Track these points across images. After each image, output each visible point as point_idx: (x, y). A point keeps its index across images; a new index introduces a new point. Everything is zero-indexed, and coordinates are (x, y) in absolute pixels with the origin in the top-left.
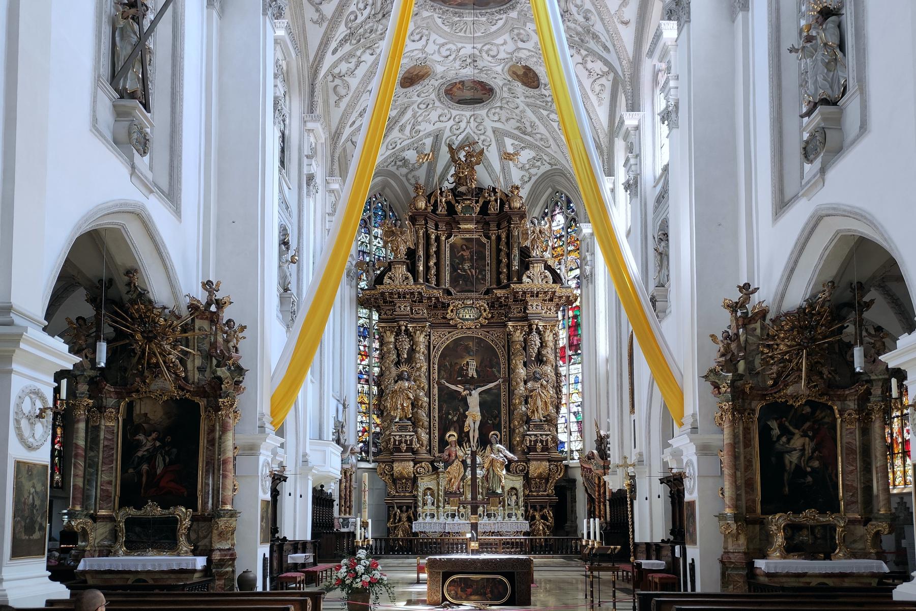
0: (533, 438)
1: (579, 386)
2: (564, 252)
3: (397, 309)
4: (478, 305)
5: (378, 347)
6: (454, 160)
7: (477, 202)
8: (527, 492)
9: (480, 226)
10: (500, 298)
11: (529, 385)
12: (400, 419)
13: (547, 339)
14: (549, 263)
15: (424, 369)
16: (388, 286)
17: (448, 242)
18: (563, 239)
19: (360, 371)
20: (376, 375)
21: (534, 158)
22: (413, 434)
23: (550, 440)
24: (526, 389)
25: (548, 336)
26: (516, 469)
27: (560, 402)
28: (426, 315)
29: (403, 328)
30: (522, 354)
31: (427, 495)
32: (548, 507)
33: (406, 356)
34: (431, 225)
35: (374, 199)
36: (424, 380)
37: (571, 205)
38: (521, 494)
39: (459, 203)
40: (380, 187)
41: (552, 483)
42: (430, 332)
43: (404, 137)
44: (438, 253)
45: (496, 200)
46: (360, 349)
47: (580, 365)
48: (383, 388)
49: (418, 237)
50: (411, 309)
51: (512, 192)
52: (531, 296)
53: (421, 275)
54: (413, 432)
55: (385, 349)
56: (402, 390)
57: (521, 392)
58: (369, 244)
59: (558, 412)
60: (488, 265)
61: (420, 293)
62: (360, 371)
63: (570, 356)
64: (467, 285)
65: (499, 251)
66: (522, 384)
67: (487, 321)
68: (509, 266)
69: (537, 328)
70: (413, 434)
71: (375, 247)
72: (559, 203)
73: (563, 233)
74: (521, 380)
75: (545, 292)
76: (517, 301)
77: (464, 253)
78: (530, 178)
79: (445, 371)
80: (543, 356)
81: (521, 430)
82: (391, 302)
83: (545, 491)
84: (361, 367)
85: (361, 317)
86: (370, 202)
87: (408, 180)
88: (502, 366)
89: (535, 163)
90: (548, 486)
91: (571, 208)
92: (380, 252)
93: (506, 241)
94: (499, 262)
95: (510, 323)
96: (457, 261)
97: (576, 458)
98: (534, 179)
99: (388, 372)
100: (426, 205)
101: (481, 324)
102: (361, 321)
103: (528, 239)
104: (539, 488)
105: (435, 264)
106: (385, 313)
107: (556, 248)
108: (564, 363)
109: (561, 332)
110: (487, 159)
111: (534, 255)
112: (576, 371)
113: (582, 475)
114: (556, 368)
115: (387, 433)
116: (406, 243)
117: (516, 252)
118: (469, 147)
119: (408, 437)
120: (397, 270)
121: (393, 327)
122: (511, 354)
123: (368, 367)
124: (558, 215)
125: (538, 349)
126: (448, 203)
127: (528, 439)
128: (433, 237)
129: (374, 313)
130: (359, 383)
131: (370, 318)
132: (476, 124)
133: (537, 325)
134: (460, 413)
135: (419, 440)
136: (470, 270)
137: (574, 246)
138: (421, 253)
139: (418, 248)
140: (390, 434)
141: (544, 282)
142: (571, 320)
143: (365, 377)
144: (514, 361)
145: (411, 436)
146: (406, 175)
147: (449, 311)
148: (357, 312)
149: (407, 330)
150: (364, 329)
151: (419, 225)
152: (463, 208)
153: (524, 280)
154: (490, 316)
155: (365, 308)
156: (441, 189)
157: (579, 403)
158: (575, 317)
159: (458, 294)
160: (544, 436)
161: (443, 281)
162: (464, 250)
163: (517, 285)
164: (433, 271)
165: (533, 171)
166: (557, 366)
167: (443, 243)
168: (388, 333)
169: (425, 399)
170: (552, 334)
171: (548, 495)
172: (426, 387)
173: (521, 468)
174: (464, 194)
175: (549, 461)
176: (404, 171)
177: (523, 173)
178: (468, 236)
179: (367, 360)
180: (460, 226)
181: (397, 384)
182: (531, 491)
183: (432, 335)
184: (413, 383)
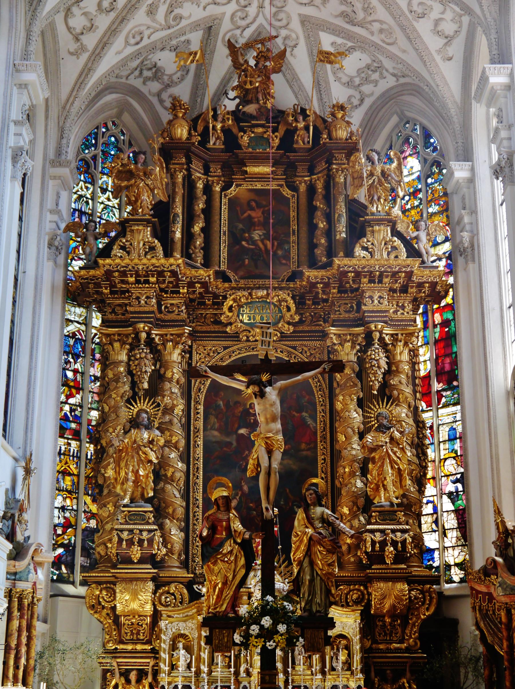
0: (378, 537)
1: (457, 445)
2: (422, 216)
3: (135, 302)
4: (276, 299)
5: (99, 374)
6: (236, 64)
7: (275, 130)
8: (368, 644)
9: (280, 171)
10: (313, 285)
11: (369, 438)
12: (132, 500)
13: (398, 358)
14: (400, 227)
15: (179, 410)
16: (118, 261)
17: (226, 196)
18: (420, 196)
19: (66, 414)
20: (94, 423)
21: (368, 67)
22: (155, 527)
23: (410, 540)
24: (363, 447)
25: (401, 353)
26: (347, 598)
27: (425, 474)
28: (184, 315)
29: (144, 335)
30: (355, 385)
31: (178, 648)
32: (408, 675)
33: (146, 386)
34: (197, 167)
35: (104, 130)
36: (178, 430)
37: (432, 141)
38: (357, 647)
39: (245, 132)
40: (115, 111)
41: (414, 625)
42: (191, 347)
43: (154, 25)
44: (208, 212)
45: (307, 128)
46: (66, 376)
47: (459, 407)
48: (104, 444)
49: (174, 184)
50: (159, 305)
51: (333, 115)
52: (370, 282)
53: (178, 246)
54: (154, 523)
55: (110, 374)
56: (137, 447)
57: (354, 452)
58: (92, 199)
59: (421, 491)
60: (294, 234)
61: (174, 273)
62: (66, 414)
63: (438, 392)
64: (256, 267)
65: (312, 209)
66: (356, 438)
67: (292, 329)
68: (329, 233)
69: (381, 339)
70: (155, 527)
71: (102, 206)
72: (411, 140)
73: (420, 187)
74: (354, 431)
75: (394, 274)
76: (345, 292)
77: (253, 214)
78: (362, 101)
79: (217, 417)
80: (394, 387)
81: (356, 523)
82: (123, 292)
83: (401, 642)
84: (67, 408)
85: (72, 321)
86: (96, 134)
87: (161, 101)
88: (319, 408)
89: (370, 76)
90: (407, 631)
91: (432, 144)
92: (111, 214)
93: (324, 192)
94: (312, 227)
95: (333, 330)
96: (241, 226)
97: (456, 578)
98: (368, 102)
99: (113, 416)
100: (189, 133)
101: (281, 333)
102: (72, 328)
103: (361, 185)
104: (391, 635)
105: (202, 230)
106: (113, 312)
107: (408, 210)
108: (429, 405)
109: (421, 351)
110: (291, 69)
111: (374, 209)
112: (450, 419)
113: (474, 608)
114: (416, 413)
115: (108, 527)
116: (152, 190)
117: (341, 208)
118: (263, 44)
119: (145, 534)
120: (136, 235)
121: (127, 336)
122: (335, 385)
123: (79, 410)
124: (409, 159)
125: (384, 374)
126: (226, 131)
127: (369, 539)
128: (200, 185)
129: (94, 315)
130: (62, 436)
131: (86, 323)
132: (274, 10)
133: (381, 332)
134: (243, 494)
135: (165, 543)
136: (262, 241)
137: (439, 204)
138: (179, 210)
139: (174, 201)
140: (112, 529)
141: (392, 256)
142: (438, 329)
143: (73, 426)
144: (341, 398)
145: (150, 531)
146: (159, 95)
147: (225, 309)
148: (64, 310)
149: (150, 342)
150: (76, 342)
151: (177, 164)
152: (251, 139)
153: (357, 254)
154: (297, 318)
155: (79, 306)
156: (215, 110)
157: (459, 476)
158: (446, 323)
159: (242, 281)
160: (399, 534)
161: (216, 259)
162: (252, 209)
163: (346, 261)
164: (199, 242)
165: (367, 89)
166: (416, 408)
167: (217, 196)
168: (117, 345)
169: (180, 464)
170: (406, 351)
171: (408, 650)
172: (182, 443)
173: (355, 597)
174: (252, 117)
175: (411, 580)
176: (155, 86)
177: (351, 92)
178: (259, 186)
179: (79, 396)
180: (248, 169)
181: (128, 435)
182: (375, 641)
183: (194, 353)
184: (157, 432)
